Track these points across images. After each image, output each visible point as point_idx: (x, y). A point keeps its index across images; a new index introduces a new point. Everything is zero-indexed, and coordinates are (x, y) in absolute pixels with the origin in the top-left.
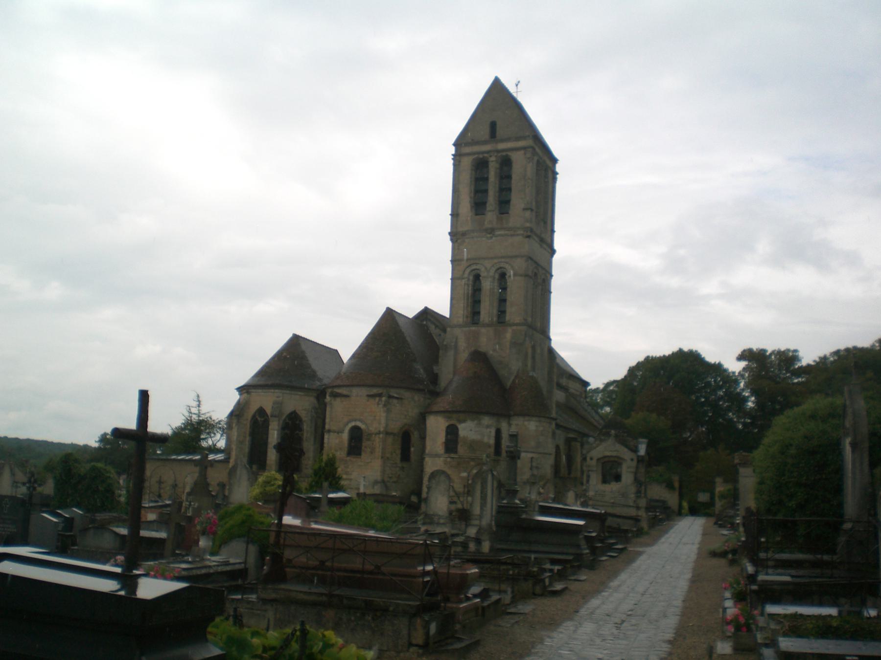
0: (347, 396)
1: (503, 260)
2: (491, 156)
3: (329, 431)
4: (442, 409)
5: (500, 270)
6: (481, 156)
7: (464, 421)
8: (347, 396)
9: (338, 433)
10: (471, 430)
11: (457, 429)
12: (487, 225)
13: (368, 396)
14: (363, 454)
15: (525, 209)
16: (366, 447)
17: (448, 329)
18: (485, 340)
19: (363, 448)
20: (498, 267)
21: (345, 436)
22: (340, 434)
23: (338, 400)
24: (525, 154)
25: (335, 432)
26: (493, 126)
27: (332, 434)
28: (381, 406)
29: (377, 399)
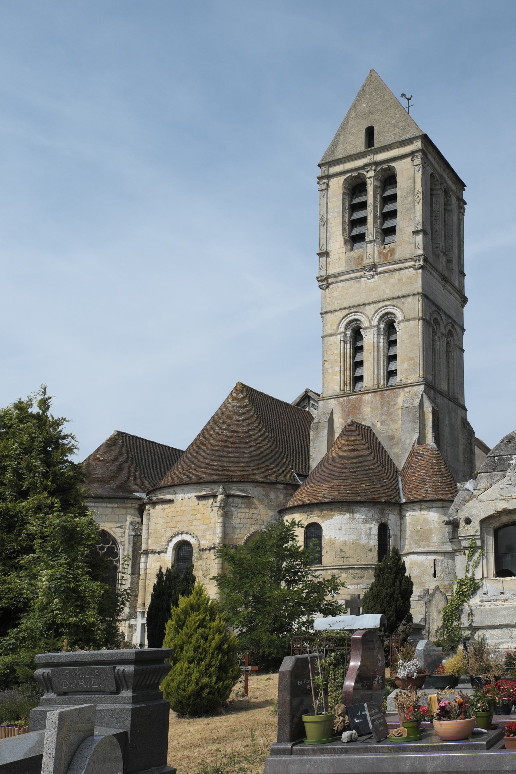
0: (171, 501)
1: (388, 303)
2: (367, 172)
3: (146, 553)
4: (298, 503)
5: (386, 317)
6: (355, 174)
7: (329, 517)
8: (171, 501)
9: (159, 553)
10: (340, 528)
11: (321, 528)
12: (368, 261)
13: (199, 498)
15: (415, 233)
20: (383, 312)
22: (162, 554)
23: (158, 507)
25: (155, 553)
26: (370, 132)
27: (150, 555)
28: (215, 509)
29: (211, 501)
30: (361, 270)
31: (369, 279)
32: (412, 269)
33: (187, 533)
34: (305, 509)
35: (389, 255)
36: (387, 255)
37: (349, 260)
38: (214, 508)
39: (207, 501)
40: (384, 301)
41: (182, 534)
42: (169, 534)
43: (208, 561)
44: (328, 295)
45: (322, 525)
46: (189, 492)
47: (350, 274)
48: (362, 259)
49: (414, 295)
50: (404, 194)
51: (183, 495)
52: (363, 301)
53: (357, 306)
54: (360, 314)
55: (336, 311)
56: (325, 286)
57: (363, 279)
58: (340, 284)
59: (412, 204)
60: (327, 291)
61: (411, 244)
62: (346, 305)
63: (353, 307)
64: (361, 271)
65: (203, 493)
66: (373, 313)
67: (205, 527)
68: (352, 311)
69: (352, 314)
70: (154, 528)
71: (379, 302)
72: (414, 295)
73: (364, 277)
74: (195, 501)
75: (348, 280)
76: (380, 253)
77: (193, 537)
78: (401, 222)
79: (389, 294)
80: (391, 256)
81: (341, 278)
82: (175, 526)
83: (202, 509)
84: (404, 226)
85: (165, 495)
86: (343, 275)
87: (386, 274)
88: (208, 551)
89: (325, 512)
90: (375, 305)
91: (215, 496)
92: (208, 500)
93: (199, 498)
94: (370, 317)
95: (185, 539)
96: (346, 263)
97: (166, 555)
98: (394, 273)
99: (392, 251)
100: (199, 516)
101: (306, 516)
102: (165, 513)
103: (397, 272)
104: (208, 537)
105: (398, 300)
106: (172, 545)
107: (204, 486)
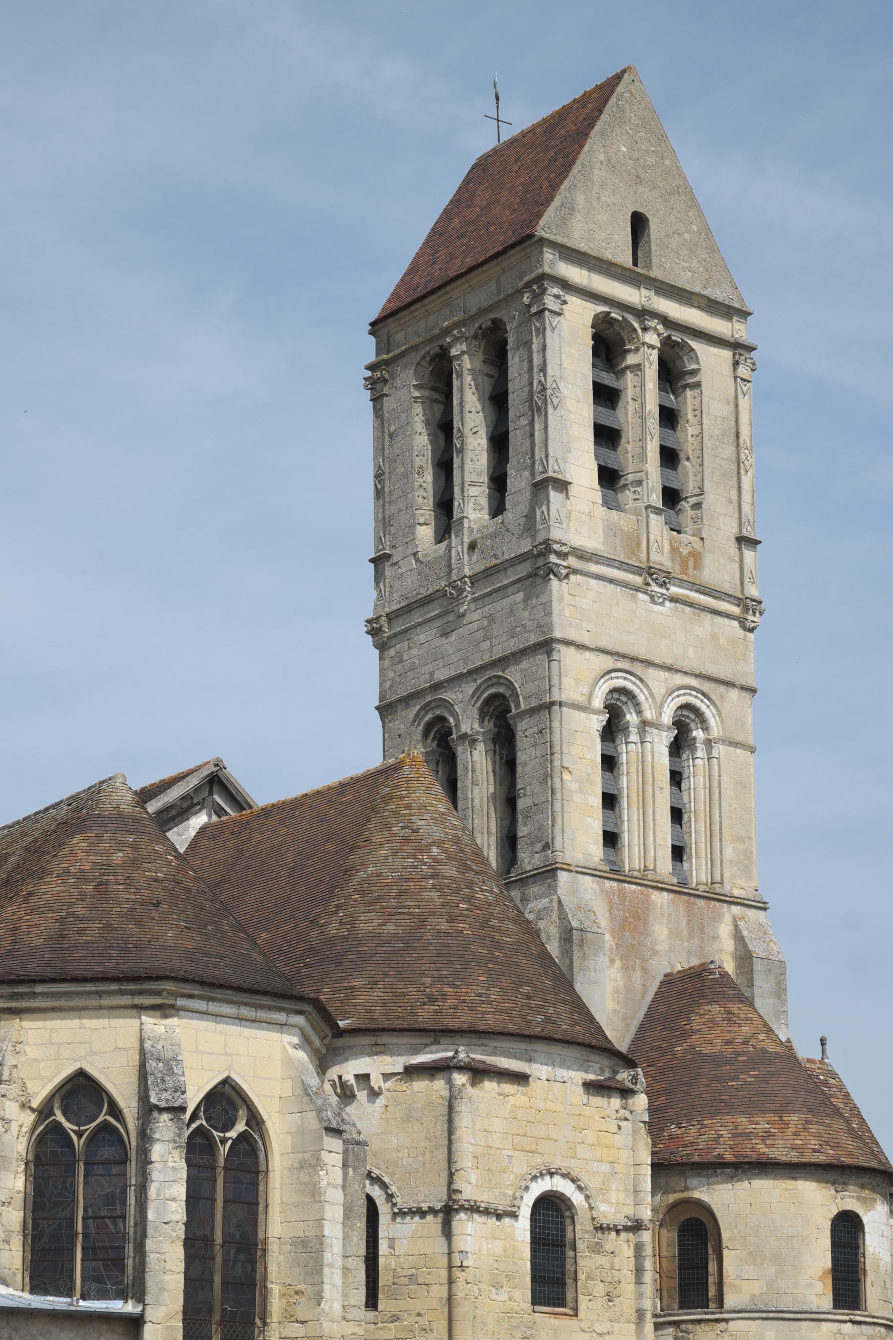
1: (693, 682)
8: (521, 1078)
9: (499, 1217)
14: (583, 1303)
16: (589, 1277)
17: (563, 876)
18: (665, 932)
19: (582, 1277)
21: (522, 1228)
22: (507, 1220)
23: (490, 1086)
24: (736, 364)
29: (616, 1102)
30: (637, 571)
31: (653, 601)
32: (735, 624)
33: (565, 1176)
34: (833, 1176)
35: (691, 563)
36: (687, 562)
37: (611, 531)
38: (623, 1124)
39: (606, 1099)
40: (686, 673)
41: (552, 1174)
42: (521, 1166)
43: (617, 1260)
44: (567, 597)
45: (865, 1220)
46: (563, 1064)
47: (612, 566)
48: (639, 544)
49: (743, 688)
50: (717, 432)
51: (550, 1068)
52: (641, 651)
53: (634, 659)
54: (638, 682)
55: (587, 648)
56: (564, 572)
57: (641, 596)
58: (593, 582)
59: (734, 467)
60: (564, 584)
61: (731, 560)
62: (604, 643)
63: (624, 656)
64: (634, 573)
65: (591, 1077)
66: (663, 691)
67: (605, 1168)
68: (620, 665)
69: (620, 674)
70: (483, 1143)
71: (677, 671)
72: (743, 688)
73: (645, 593)
74: (578, 1094)
75: (611, 581)
76: (674, 550)
77: (580, 1188)
78: (711, 496)
79: (692, 659)
80: (695, 568)
81: (594, 568)
82: (534, 1147)
83: (597, 1117)
84: (719, 510)
85: (493, 1054)
86: (597, 563)
87: (688, 609)
88: (613, 1234)
89: (867, 1191)
90: (666, 674)
91: (626, 1093)
92: (609, 1097)
93: (591, 1087)
94: (659, 700)
95: (561, 1189)
96: (606, 535)
97: (515, 1223)
98: (703, 614)
99: (696, 556)
100: (590, 1136)
101: (834, 1193)
102: (508, 1105)
103: (709, 616)
104: (613, 1197)
105: (712, 685)
106: (529, 1199)
107: (594, 1057)
